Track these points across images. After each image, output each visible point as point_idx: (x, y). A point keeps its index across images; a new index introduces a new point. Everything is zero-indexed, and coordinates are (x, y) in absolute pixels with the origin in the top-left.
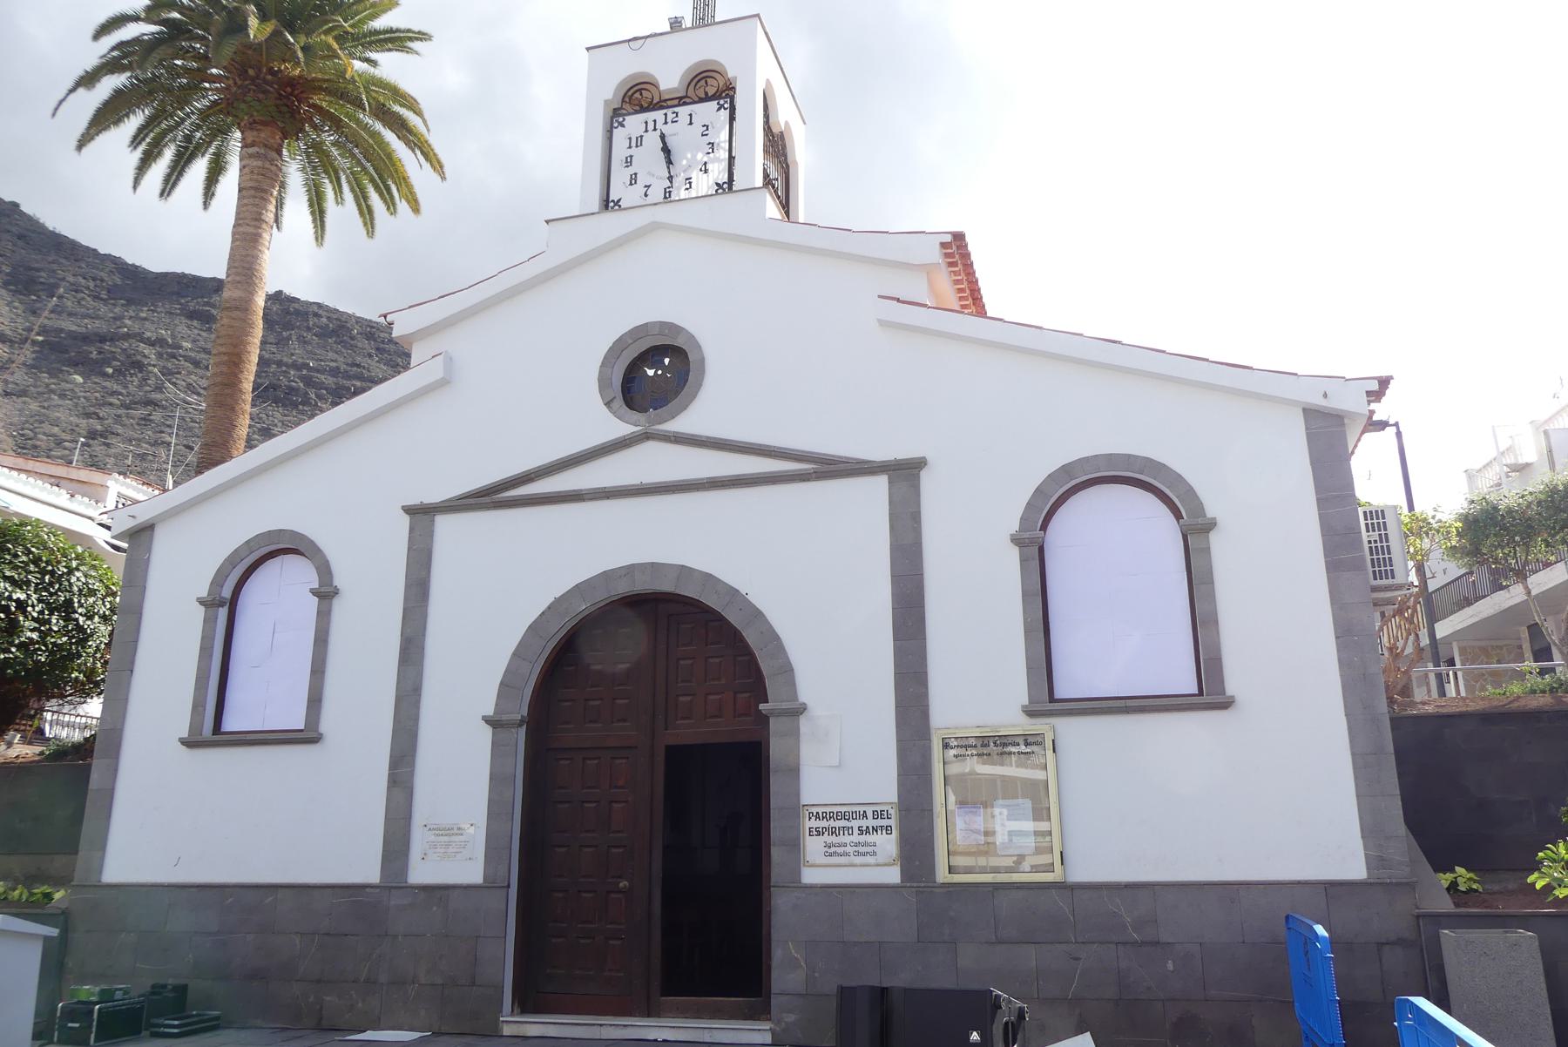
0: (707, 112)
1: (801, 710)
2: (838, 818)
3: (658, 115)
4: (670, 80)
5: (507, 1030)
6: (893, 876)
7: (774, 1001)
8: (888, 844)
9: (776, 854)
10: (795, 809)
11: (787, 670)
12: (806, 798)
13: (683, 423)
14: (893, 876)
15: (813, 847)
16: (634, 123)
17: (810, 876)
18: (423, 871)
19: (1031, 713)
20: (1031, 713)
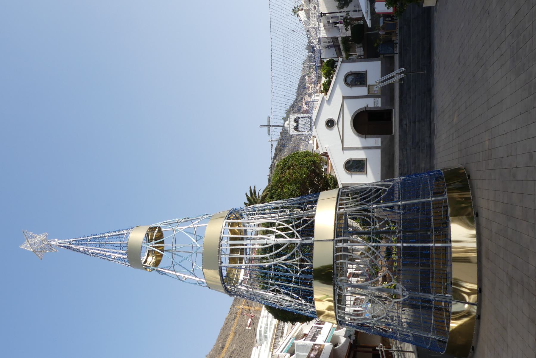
0: (300, 120)
1: (365, 107)
2: (375, 103)
3: (299, 126)
4: (295, 124)
5: (394, 134)
6: (380, 99)
7: (391, 109)
8: (377, 99)
9: (378, 109)
10: (374, 107)
11: (361, 108)
12: (373, 106)
13: (336, 121)
14: (380, 99)
15: (378, 106)
16: (300, 129)
17: (380, 106)
18: (380, 145)
19: (366, 87)
20: (366, 87)
